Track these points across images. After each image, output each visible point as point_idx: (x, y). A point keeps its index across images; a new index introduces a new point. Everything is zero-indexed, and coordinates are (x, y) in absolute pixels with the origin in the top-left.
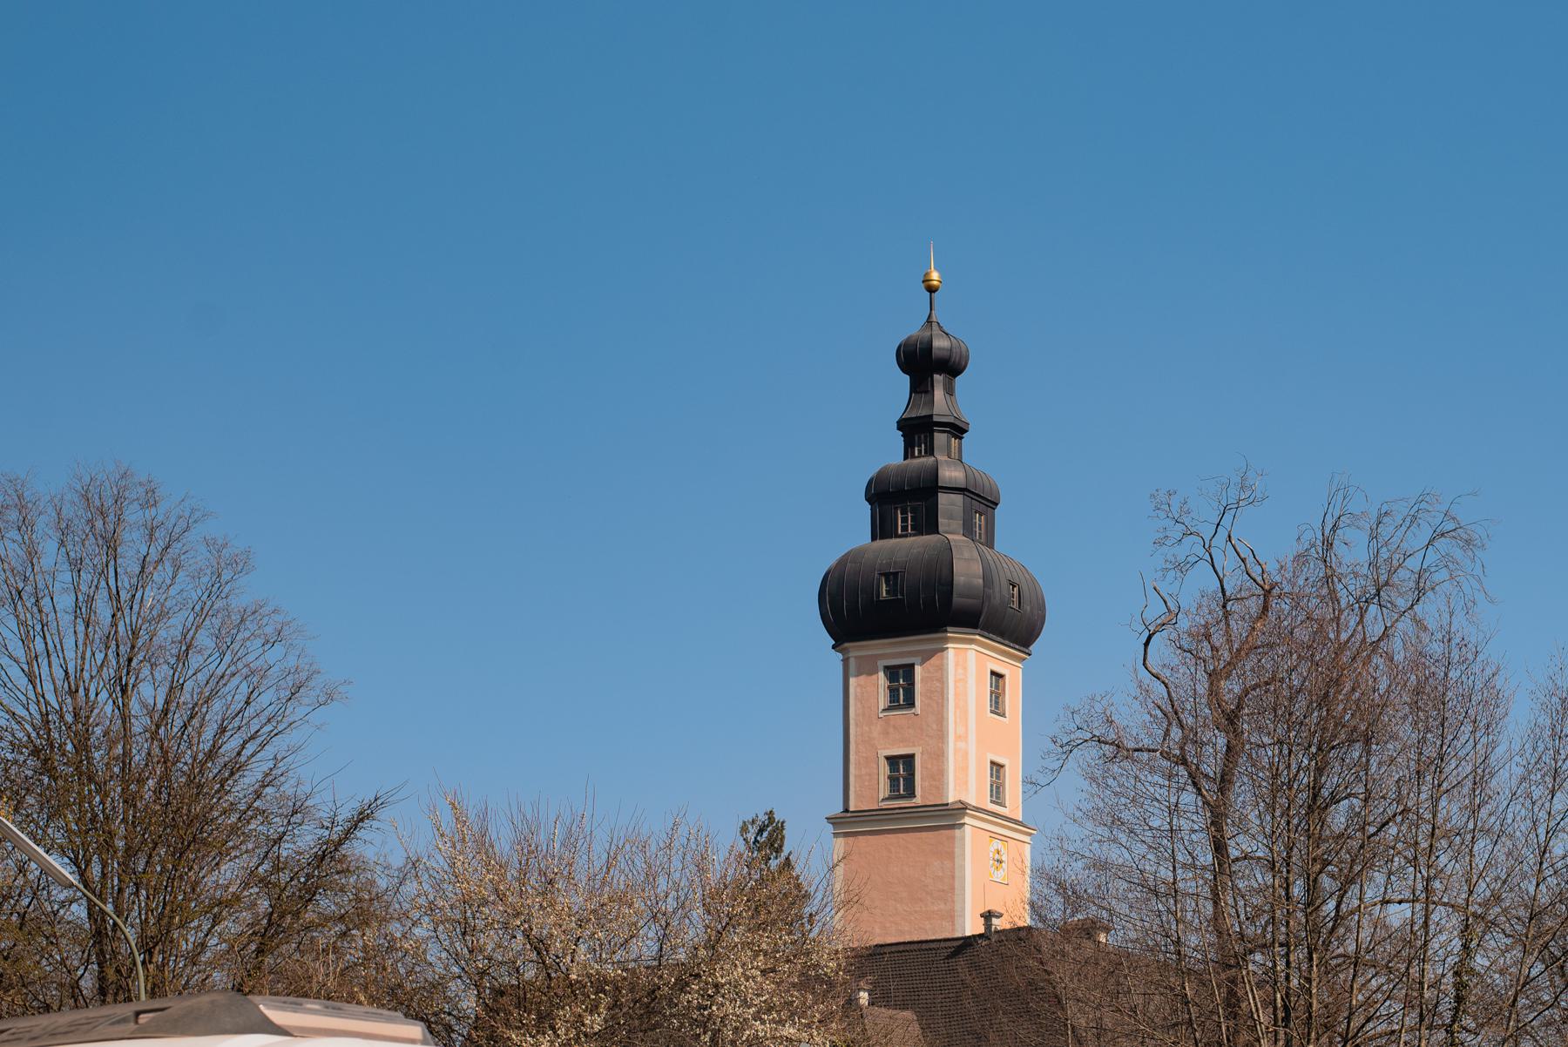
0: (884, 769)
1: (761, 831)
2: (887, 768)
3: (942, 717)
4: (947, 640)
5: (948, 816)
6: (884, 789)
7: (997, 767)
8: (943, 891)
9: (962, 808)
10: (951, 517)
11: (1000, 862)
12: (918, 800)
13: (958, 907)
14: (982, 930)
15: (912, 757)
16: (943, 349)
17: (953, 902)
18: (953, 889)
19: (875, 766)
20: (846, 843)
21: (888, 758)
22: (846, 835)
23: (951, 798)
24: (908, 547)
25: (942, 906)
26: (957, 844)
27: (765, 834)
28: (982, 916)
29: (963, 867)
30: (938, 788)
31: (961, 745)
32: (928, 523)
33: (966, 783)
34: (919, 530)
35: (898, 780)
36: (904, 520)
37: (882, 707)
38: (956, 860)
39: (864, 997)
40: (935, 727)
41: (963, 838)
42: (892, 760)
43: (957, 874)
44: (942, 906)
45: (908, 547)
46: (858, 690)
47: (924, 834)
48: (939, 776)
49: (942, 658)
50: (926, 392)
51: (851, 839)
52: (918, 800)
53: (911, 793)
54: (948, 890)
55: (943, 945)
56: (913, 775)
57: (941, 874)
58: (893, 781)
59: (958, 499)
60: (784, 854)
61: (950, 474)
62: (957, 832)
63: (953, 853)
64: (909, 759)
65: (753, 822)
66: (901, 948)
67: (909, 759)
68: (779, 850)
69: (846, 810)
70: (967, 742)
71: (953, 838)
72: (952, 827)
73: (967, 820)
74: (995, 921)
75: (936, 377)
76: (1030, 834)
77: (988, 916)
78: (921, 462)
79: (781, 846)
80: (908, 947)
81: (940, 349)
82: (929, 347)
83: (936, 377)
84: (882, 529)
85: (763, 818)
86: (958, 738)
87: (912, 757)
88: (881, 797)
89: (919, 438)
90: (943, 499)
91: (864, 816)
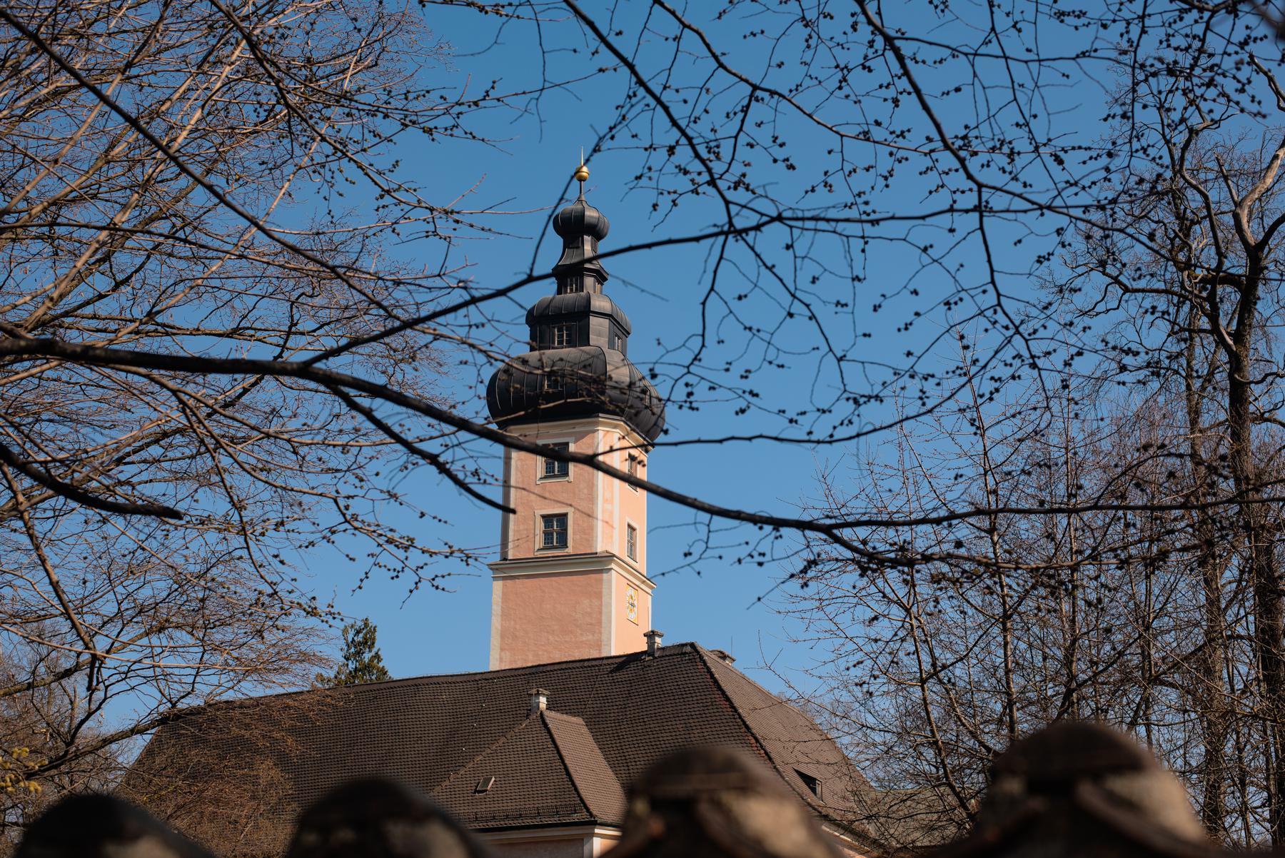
0: (540, 525)
1: (358, 632)
2: (543, 524)
3: (593, 484)
4: (598, 424)
5: (598, 563)
6: (539, 541)
7: (632, 528)
8: (591, 624)
9: (611, 557)
10: (599, 335)
11: (632, 605)
12: (570, 550)
13: (604, 638)
14: (645, 648)
15: (565, 515)
16: (592, 217)
17: (600, 633)
18: (600, 622)
19: (532, 523)
20: (505, 586)
21: (543, 517)
22: (504, 578)
23: (600, 548)
24: (562, 354)
25: (590, 637)
26: (605, 586)
27: (361, 635)
28: (645, 635)
29: (610, 604)
30: (587, 540)
31: (608, 506)
32: (582, 337)
33: (612, 537)
34: (571, 344)
35: (552, 534)
36: (561, 336)
37: (539, 476)
38: (604, 599)
39: (543, 701)
40: (585, 491)
41: (610, 581)
42: (547, 519)
43: (604, 610)
44: (590, 637)
45: (562, 354)
46: (519, 463)
47: (575, 578)
48: (589, 532)
49: (593, 438)
50: (578, 248)
51: (509, 582)
52: (570, 550)
53: (563, 543)
54: (597, 623)
55: (605, 662)
56: (566, 530)
57: (589, 610)
58: (548, 535)
59: (606, 322)
60: (374, 650)
61: (599, 303)
62: (605, 576)
63: (601, 592)
64: (562, 518)
65: (352, 626)
66: (564, 666)
67: (562, 518)
68: (370, 648)
69: (505, 559)
70: (612, 504)
71: (601, 581)
72: (601, 571)
73: (613, 566)
74: (658, 640)
75: (586, 237)
76: (652, 588)
77: (651, 636)
78: (570, 296)
79: (373, 643)
80: (570, 665)
81: (590, 216)
82: (582, 216)
83: (586, 237)
84: (539, 340)
85: (360, 624)
86: (605, 501)
87: (565, 515)
88: (537, 547)
89: (571, 281)
90: (594, 321)
91: (520, 563)
